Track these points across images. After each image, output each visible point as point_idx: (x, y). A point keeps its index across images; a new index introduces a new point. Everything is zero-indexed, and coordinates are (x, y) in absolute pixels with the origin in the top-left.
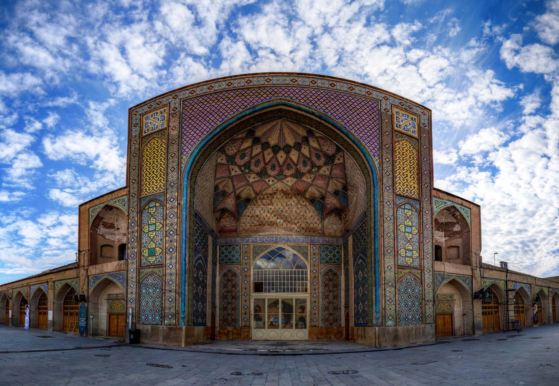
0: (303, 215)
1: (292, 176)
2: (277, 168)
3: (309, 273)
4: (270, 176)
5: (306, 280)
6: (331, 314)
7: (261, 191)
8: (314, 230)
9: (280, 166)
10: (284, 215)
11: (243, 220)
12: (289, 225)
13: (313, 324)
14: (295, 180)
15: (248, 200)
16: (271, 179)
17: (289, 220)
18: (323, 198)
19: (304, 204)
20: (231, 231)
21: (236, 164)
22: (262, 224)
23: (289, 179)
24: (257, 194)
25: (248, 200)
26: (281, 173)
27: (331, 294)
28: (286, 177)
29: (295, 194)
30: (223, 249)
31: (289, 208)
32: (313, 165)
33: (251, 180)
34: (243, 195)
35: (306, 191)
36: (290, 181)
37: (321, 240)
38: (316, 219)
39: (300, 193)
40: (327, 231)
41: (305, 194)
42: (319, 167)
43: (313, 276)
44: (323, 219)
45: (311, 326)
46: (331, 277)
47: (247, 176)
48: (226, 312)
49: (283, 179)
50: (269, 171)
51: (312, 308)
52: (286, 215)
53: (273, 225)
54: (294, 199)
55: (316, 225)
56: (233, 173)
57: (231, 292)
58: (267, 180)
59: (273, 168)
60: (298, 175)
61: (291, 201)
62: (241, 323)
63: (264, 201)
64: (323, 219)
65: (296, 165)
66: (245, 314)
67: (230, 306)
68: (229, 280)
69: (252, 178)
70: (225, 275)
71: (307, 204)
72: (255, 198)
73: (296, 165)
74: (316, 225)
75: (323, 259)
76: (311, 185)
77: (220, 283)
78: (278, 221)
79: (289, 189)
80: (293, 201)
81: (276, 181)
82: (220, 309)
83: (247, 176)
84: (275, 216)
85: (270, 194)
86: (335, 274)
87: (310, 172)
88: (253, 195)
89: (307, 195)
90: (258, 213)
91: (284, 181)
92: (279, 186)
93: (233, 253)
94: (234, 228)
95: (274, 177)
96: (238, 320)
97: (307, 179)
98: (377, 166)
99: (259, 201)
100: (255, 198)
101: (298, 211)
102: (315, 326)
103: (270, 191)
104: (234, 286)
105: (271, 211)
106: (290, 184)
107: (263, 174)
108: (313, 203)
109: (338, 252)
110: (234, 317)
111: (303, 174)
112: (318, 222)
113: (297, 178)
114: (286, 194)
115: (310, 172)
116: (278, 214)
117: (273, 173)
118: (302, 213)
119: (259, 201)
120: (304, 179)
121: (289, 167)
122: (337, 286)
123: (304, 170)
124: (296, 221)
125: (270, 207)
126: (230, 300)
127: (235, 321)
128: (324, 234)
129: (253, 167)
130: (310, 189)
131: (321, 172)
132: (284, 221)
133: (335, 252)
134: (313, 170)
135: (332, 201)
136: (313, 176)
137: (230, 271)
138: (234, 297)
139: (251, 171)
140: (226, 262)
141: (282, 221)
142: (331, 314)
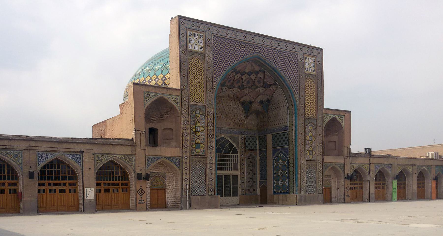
0: (236, 114)
6: (251, 186)
9: (234, 81)
10: (225, 113)
13: (242, 193)
14: (239, 90)
16: (225, 88)
18: (251, 103)
19: (237, 105)
28: (234, 87)
31: (229, 108)
32: (254, 84)
38: (243, 116)
39: (237, 98)
41: (240, 99)
44: (247, 116)
49: (232, 88)
52: (227, 112)
54: (233, 101)
60: (242, 87)
64: (247, 116)
65: (243, 82)
71: (240, 105)
73: (243, 82)
74: (243, 121)
76: (247, 95)
79: (233, 95)
81: (227, 89)
85: (221, 97)
87: (250, 88)
97: (246, 91)
108: (243, 105)
112: (244, 119)
113: (240, 89)
115: (250, 88)
118: (236, 112)
120: (244, 90)
124: (232, 118)
131: (258, 90)
134: (253, 87)
135: (256, 106)
136: (251, 90)
142: (251, 186)
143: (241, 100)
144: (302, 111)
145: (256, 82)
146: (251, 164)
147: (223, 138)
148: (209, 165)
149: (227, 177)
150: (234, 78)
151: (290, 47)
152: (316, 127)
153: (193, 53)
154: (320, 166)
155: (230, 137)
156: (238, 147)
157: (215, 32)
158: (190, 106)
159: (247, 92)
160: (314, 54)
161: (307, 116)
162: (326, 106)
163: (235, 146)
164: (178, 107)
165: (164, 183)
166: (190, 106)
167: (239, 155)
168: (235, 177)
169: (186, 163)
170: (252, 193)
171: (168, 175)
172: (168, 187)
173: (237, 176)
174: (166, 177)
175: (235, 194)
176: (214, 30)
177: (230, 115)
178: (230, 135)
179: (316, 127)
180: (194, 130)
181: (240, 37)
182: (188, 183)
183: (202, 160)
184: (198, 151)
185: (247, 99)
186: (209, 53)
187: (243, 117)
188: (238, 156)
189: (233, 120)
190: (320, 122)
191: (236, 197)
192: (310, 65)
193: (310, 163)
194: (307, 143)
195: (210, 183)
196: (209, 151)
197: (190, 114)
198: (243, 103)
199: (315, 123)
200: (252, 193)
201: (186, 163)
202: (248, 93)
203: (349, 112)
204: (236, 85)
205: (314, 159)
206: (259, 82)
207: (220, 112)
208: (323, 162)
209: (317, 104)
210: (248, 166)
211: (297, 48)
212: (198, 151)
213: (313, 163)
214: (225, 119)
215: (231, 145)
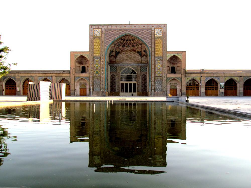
1: (131, 46)
2: (128, 44)
3: (137, 75)
4: (125, 46)
5: (136, 77)
7: (123, 50)
8: (139, 61)
11: (117, 58)
12: (131, 60)
13: (138, 91)
14: (132, 47)
15: (119, 52)
17: (131, 58)
18: (141, 52)
20: (114, 62)
21: (116, 45)
22: (123, 60)
23: (131, 47)
24: (122, 51)
25: (119, 52)
26: (129, 45)
27: (144, 82)
28: (130, 46)
29: (132, 51)
30: (111, 67)
32: (137, 44)
33: (120, 48)
34: (118, 51)
35: (136, 50)
36: (131, 47)
37: (141, 65)
38: (139, 58)
40: (143, 62)
42: (139, 45)
43: (138, 76)
44: (141, 58)
45: (138, 92)
46: (144, 76)
47: (119, 47)
48: (112, 87)
50: (125, 45)
51: (138, 86)
52: (130, 57)
53: (127, 60)
54: (133, 52)
55: (139, 60)
56: (116, 47)
57: (114, 81)
58: (125, 47)
59: (126, 44)
60: (133, 46)
61: (132, 52)
62: (117, 91)
63: (124, 53)
64: (141, 58)
66: (118, 88)
67: (113, 86)
68: (113, 77)
69: (120, 47)
70: (112, 76)
71: (137, 53)
72: (121, 52)
75: (142, 71)
76: (137, 49)
77: (110, 78)
78: (128, 59)
79: (131, 49)
80: (132, 53)
81: (127, 47)
82: (110, 86)
83: (119, 47)
84: (127, 57)
86: (145, 76)
88: (121, 51)
89: (136, 51)
90: (122, 56)
91: (130, 47)
92: (128, 48)
93: (114, 69)
94: (115, 61)
95: (127, 46)
96: (116, 90)
98: (150, 50)
99: (122, 52)
100: (121, 52)
101: (134, 55)
102: (139, 92)
103: (125, 50)
104: (115, 79)
105: (126, 56)
106: (131, 48)
107: (124, 46)
109: (146, 68)
110: (114, 89)
111: (135, 46)
114: (130, 51)
115: (136, 46)
116: (128, 57)
117: (126, 45)
119: (122, 52)
120: (135, 47)
121: (131, 44)
122: (146, 79)
123: (135, 45)
125: (125, 54)
126: (113, 84)
127: (115, 90)
128: (142, 62)
129: (121, 45)
130: (137, 50)
132: (130, 59)
133: (145, 68)
137: (113, 74)
138: (115, 83)
139: (120, 46)
140: (112, 72)
141: (129, 59)
142: (144, 88)
143: (136, 51)
144: (153, 54)
145: (137, 43)
146: (144, 78)
147: (129, 68)
148: (102, 80)
149: (131, 84)
150: (128, 43)
151: (146, 27)
152: (162, 61)
153: (96, 37)
154: (164, 79)
155: (132, 67)
156: (136, 71)
157: (106, 27)
158: (93, 57)
159: (137, 47)
160: (161, 27)
161: (156, 56)
162: (168, 50)
163: (135, 71)
164: (88, 58)
165: (86, 87)
166: (93, 57)
167: (137, 74)
168: (135, 85)
169: (91, 79)
170: (144, 91)
171: (87, 84)
172: (87, 88)
173: (136, 84)
174: (86, 84)
175: (135, 91)
176: (105, 27)
177: (132, 58)
178: (132, 66)
179: (162, 61)
180: (95, 66)
181: (118, 27)
182: (92, 87)
183: (98, 77)
184: (97, 74)
185: (138, 50)
186: (103, 36)
187: (139, 58)
188: (136, 75)
189: (134, 60)
190: (164, 58)
191: (135, 93)
192: (158, 33)
193: (158, 78)
194: (158, 68)
195: (102, 86)
196: (102, 74)
197: (94, 60)
198: (138, 52)
199: (162, 59)
200: (144, 91)
201: (91, 79)
202: (137, 48)
203: (185, 52)
204: (130, 45)
205: (161, 75)
206: (138, 43)
207: (127, 57)
208: (166, 77)
209: (163, 50)
210: (142, 79)
211: (150, 26)
212: (97, 74)
213: (160, 77)
214: (130, 60)
215: (133, 71)
